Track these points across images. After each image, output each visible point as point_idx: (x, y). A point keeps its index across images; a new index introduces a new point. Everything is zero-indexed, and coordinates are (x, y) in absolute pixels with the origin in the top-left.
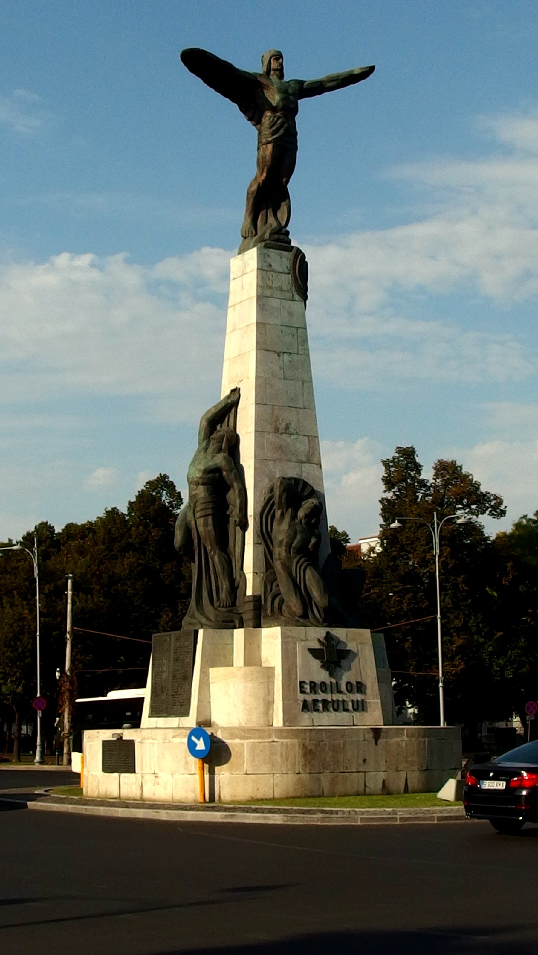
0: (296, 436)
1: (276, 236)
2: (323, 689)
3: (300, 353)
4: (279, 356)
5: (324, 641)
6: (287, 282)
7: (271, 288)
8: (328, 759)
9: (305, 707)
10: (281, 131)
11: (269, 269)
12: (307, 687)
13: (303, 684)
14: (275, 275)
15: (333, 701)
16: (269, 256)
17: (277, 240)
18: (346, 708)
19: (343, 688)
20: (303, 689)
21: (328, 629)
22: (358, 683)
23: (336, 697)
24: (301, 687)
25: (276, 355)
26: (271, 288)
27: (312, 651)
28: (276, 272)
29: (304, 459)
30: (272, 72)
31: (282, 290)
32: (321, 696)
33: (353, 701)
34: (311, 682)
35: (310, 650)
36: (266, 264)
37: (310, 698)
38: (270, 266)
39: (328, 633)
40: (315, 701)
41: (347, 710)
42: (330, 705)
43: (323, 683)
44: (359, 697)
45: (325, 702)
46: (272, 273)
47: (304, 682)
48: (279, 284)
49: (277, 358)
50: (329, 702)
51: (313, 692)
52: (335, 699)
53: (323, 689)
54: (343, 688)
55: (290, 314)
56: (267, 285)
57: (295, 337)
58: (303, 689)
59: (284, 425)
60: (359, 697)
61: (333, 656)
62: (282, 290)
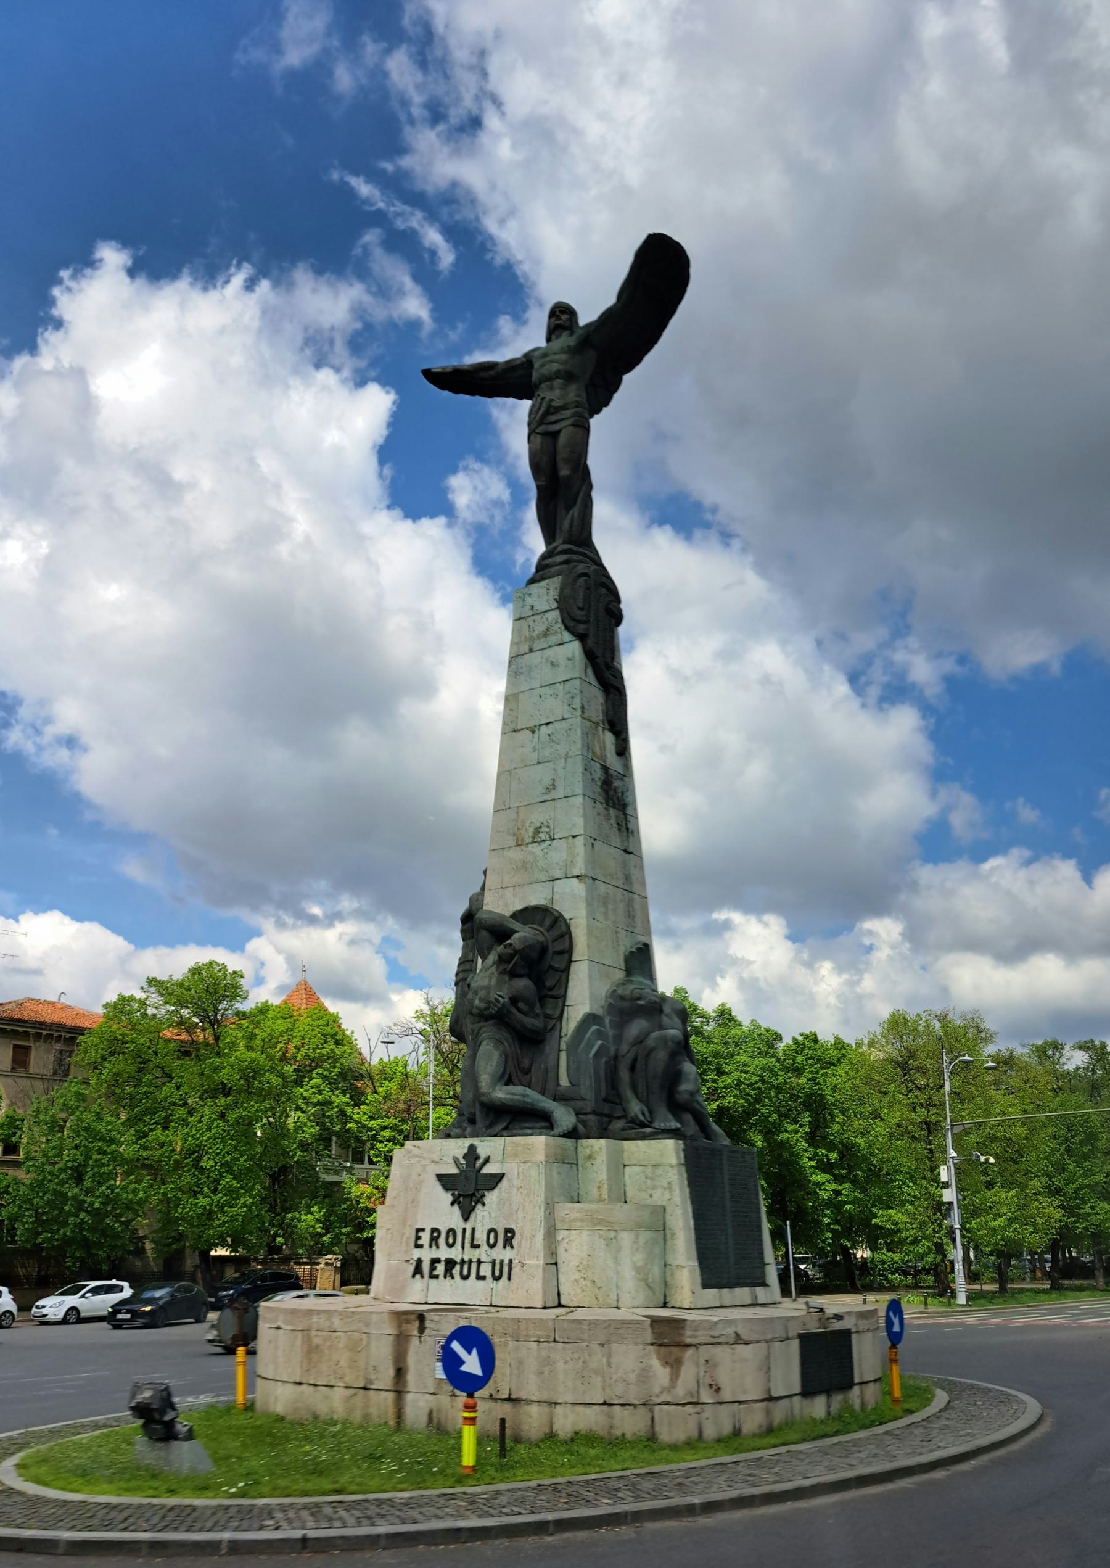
0: (547, 843)
2: (451, 1241)
4: (533, 732)
5: (463, 1162)
8: (343, 1363)
9: (418, 1270)
12: (425, 1238)
13: (420, 1234)
15: (463, 1262)
18: (482, 1273)
19: (481, 1237)
20: (420, 1242)
21: (476, 1141)
22: (508, 1230)
23: (469, 1254)
24: (418, 1238)
25: (529, 733)
27: (441, 1177)
29: (558, 874)
32: (444, 1253)
33: (494, 1262)
34: (434, 1230)
35: (441, 1177)
37: (426, 1255)
38: (532, 607)
39: (472, 1148)
40: (435, 1261)
41: (480, 1278)
42: (458, 1267)
43: (451, 1231)
44: (506, 1255)
45: (450, 1264)
47: (423, 1230)
50: (456, 1263)
51: (434, 1247)
52: (466, 1259)
53: (451, 1241)
54: (481, 1237)
58: (420, 1242)
59: (531, 830)
60: (506, 1255)
61: (469, 1187)
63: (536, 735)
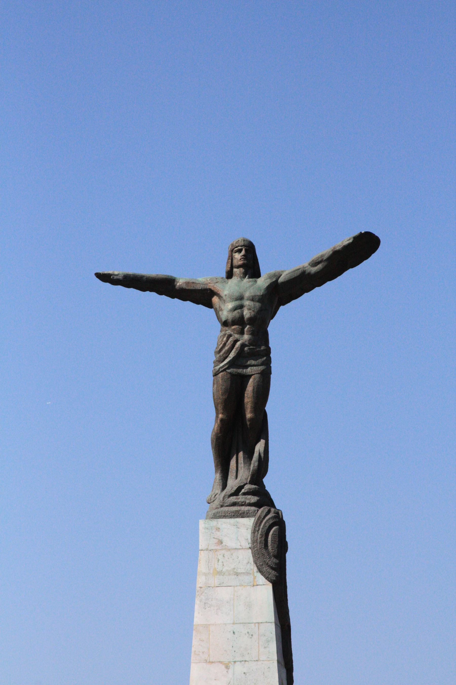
1: (233, 499)
3: (261, 659)
4: (227, 667)
6: (245, 562)
7: (220, 573)
10: (232, 355)
11: (218, 548)
14: (227, 554)
16: (218, 529)
17: (234, 504)
25: (223, 667)
26: (220, 573)
28: (229, 550)
30: (235, 270)
31: (237, 574)
36: (216, 541)
38: (222, 543)
46: (223, 552)
48: (232, 566)
49: (226, 670)
55: (249, 606)
56: (215, 569)
57: (255, 636)
62: (237, 574)
63: (231, 671)
